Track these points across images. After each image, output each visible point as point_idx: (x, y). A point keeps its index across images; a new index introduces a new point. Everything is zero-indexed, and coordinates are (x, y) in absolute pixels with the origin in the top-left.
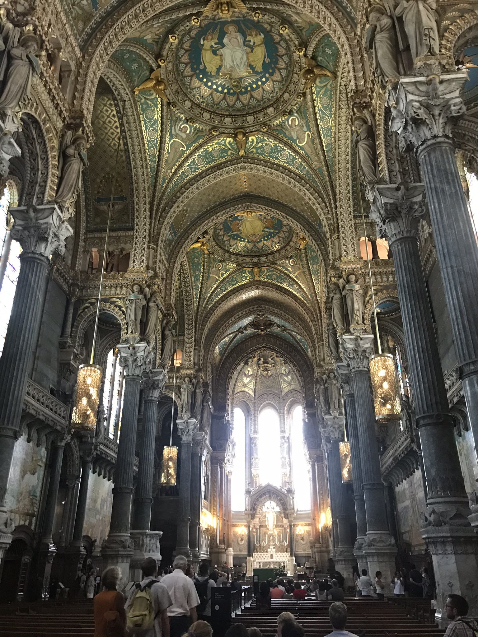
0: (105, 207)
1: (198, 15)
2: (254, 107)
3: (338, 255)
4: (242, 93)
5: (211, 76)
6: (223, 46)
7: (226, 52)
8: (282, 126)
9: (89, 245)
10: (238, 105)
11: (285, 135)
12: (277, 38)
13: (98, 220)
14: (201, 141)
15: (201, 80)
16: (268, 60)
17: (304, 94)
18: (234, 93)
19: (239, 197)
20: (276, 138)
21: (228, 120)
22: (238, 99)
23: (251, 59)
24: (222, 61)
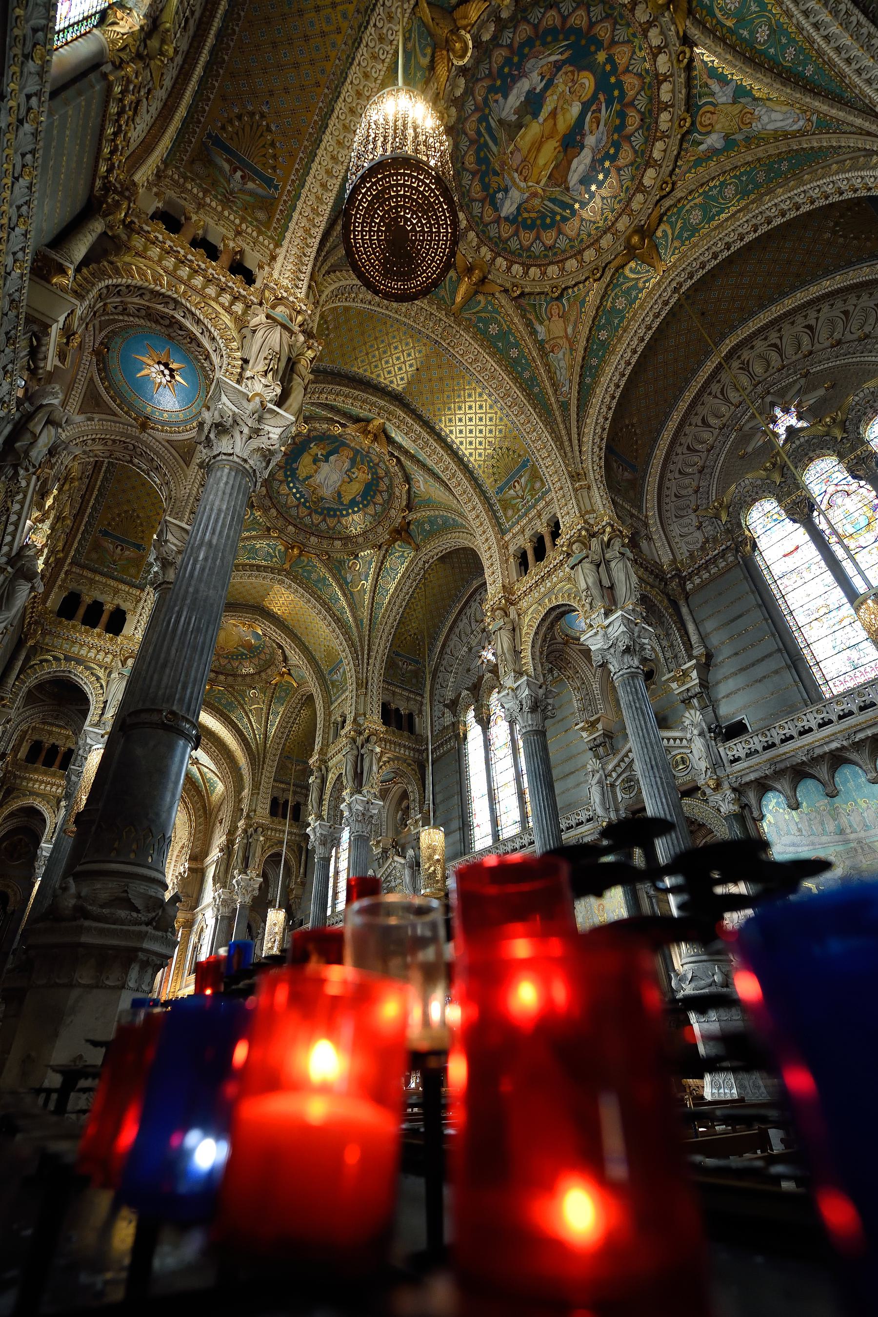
0: (111, 546)
1: (343, 426)
2: (322, 531)
3: (362, 711)
4: (316, 512)
5: (297, 479)
6: (327, 461)
7: (325, 468)
8: (341, 562)
9: (71, 581)
10: (307, 520)
11: (340, 572)
12: (383, 486)
13: (94, 556)
14: (254, 533)
15: (286, 476)
16: (359, 499)
17: (380, 547)
18: (309, 508)
19: (252, 606)
20: (330, 570)
21: (291, 528)
22: (310, 515)
23: (343, 488)
24: (316, 472)
